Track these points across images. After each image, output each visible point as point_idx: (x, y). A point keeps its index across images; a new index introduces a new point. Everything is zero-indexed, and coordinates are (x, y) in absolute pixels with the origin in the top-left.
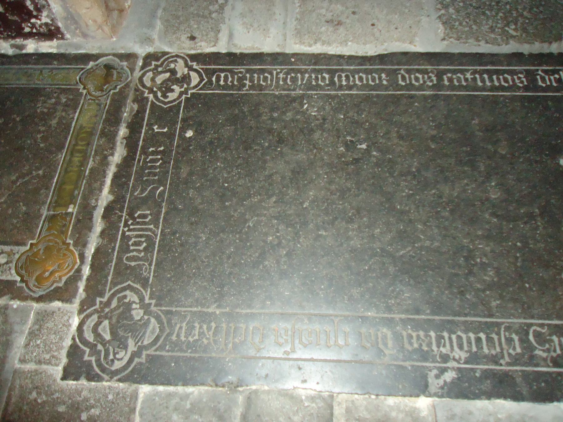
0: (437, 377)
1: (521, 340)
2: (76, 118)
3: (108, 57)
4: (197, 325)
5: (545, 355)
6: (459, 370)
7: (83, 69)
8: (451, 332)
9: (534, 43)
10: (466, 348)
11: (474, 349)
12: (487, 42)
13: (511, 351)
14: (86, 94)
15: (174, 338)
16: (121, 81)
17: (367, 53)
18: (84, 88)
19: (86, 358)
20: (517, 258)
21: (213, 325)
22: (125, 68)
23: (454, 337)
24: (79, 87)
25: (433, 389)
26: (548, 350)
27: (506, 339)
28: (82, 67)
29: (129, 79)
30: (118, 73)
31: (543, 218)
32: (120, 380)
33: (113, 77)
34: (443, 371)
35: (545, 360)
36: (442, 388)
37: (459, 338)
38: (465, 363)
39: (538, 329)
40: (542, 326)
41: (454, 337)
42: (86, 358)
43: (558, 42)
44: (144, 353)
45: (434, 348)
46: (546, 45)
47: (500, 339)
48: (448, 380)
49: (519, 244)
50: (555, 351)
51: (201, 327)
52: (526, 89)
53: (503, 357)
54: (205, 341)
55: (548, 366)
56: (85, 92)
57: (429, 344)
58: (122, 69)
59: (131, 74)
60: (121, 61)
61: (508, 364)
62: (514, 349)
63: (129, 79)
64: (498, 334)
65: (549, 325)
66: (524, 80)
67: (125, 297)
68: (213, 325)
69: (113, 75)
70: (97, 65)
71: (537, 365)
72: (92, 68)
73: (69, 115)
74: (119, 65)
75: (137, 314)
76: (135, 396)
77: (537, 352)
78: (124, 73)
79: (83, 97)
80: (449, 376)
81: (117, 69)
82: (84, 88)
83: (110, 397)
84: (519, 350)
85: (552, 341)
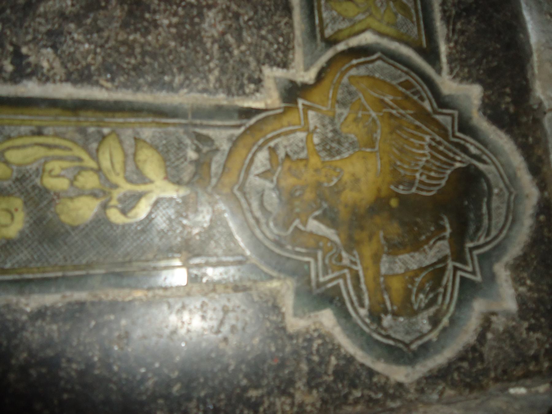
2: (31, 88)
3: (526, 179)
7: (431, 54)
14: (248, 113)
16: (375, 316)
18: (293, 92)
22: (479, 306)
24: (298, 56)
28: (443, 48)
29: (400, 374)
30: (436, 273)
33: (394, 248)
56: (268, 99)
58: (469, 289)
59: (441, 375)
60: (518, 267)
63: (400, 374)
69: (416, 246)
70: (466, 127)
72: (443, 102)
73: (54, 38)
74: (487, 260)
78: (435, 321)
79: (221, 99)
81: (459, 255)
82: (293, 92)
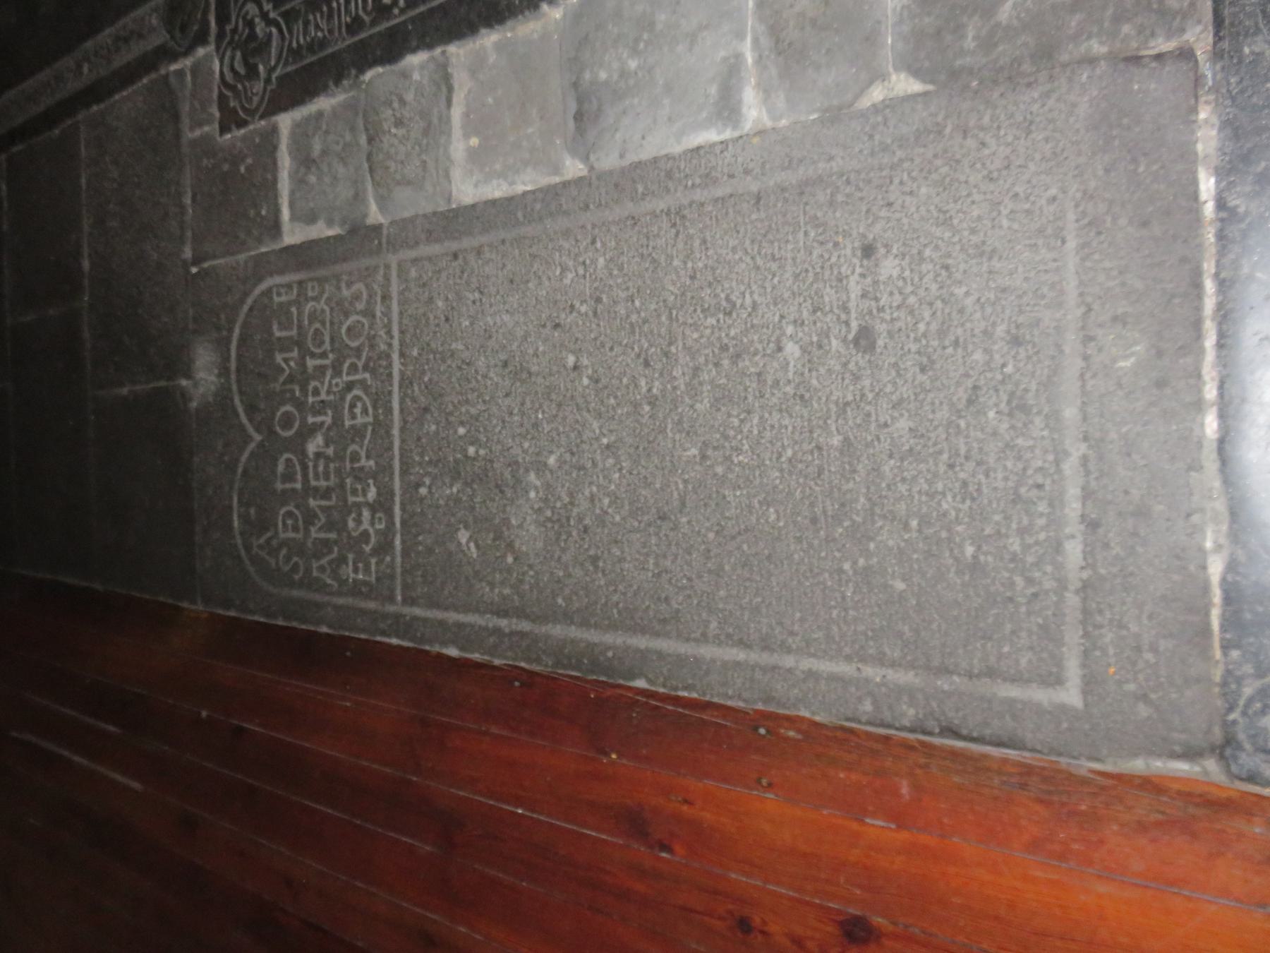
4: (311, 17)
15: (295, 45)
19: (232, 104)
21: (325, 9)
32: (262, 117)
42: (232, 104)
44: (274, 76)
51: (315, 19)
54: (320, 34)
67: (247, 13)
68: (325, 9)
75: (260, 28)
76: (274, 130)
83: (257, 140)
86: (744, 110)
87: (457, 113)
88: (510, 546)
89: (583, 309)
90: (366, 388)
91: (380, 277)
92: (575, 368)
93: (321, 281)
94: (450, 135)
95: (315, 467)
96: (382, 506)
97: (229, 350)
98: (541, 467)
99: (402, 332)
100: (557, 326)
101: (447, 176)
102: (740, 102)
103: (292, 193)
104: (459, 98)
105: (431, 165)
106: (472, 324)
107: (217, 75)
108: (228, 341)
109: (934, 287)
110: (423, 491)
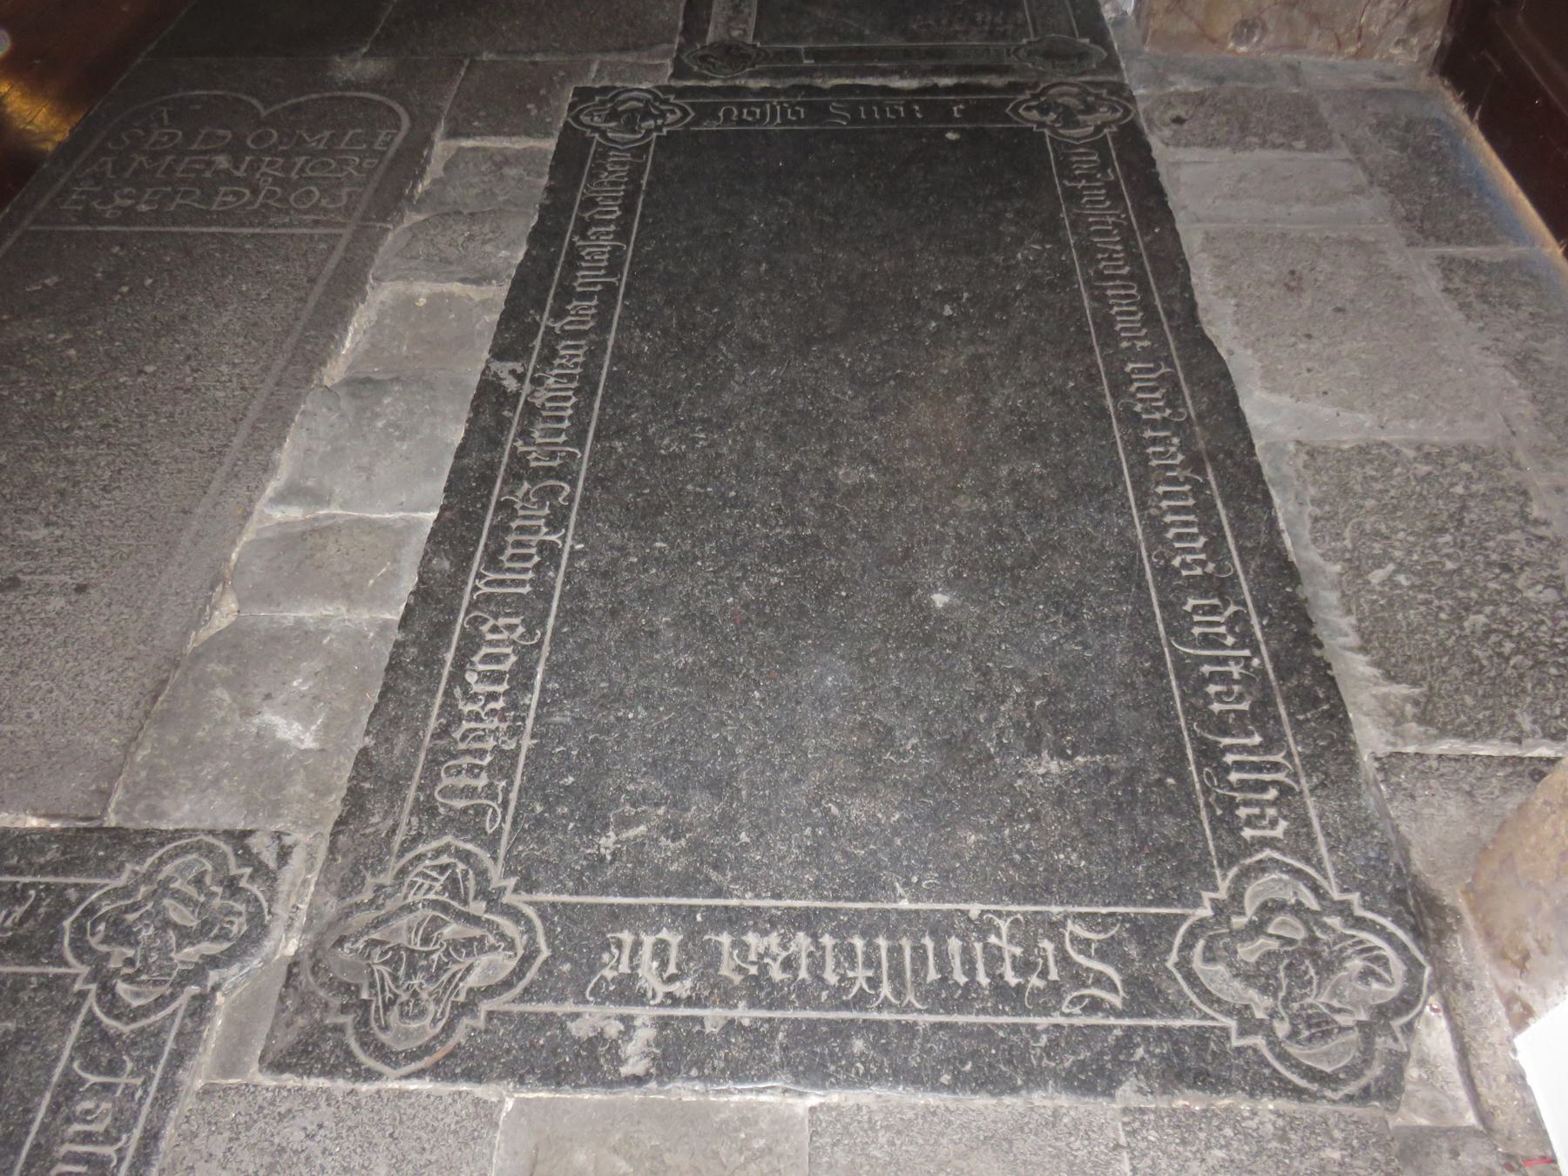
0: (513, 372)
1: (551, 468)
5: (520, 494)
6: (517, 394)
8: (577, 391)
9: (1349, 612)
10: (548, 405)
11: (544, 414)
12: (1316, 520)
13: (534, 455)
17: (1209, 322)
20: (703, 486)
23: (570, 393)
25: (496, 366)
26: (526, 497)
27: (554, 452)
31: (790, 537)
34: (520, 378)
35: (512, 493)
36: (495, 375)
37: (567, 399)
38: (526, 402)
39: (565, 494)
40: (570, 498)
41: (570, 393)
43: (1376, 672)
45: (556, 371)
46: (1353, 640)
47: (556, 444)
48: (505, 383)
49: (733, 494)
50: (523, 508)
52: (1165, 572)
53: (526, 444)
55: (500, 496)
57: (561, 366)
61: (514, 449)
62: (537, 459)
64: (565, 443)
65: (569, 508)
66: (1198, 571)
71: (505, 482)
77: (526, 485)
80: (511, 384)
84: (533, 464)
85: (542, 507)
86: (282, 507)
87: (456, 288)
88: (18, 317)
89: (189, 380)
90: (251, 203)
91: (339, 218)
92: (141, 372)
93: (371, 172)
94: (436, 281)
95: (200, 162)
96: (128, 216)
97: (365, 90)
98: (69, 344)
99: (275, 236)
100: (188, 358)
101: (399, 278)
102: (290, 504)
103: (484, 149)
104: (471, 290)
105: (413, 264)
106: (241, 292)
107: (630, 86)
108: (374, 91)
109: (16, 634)
110: (116, 249)
